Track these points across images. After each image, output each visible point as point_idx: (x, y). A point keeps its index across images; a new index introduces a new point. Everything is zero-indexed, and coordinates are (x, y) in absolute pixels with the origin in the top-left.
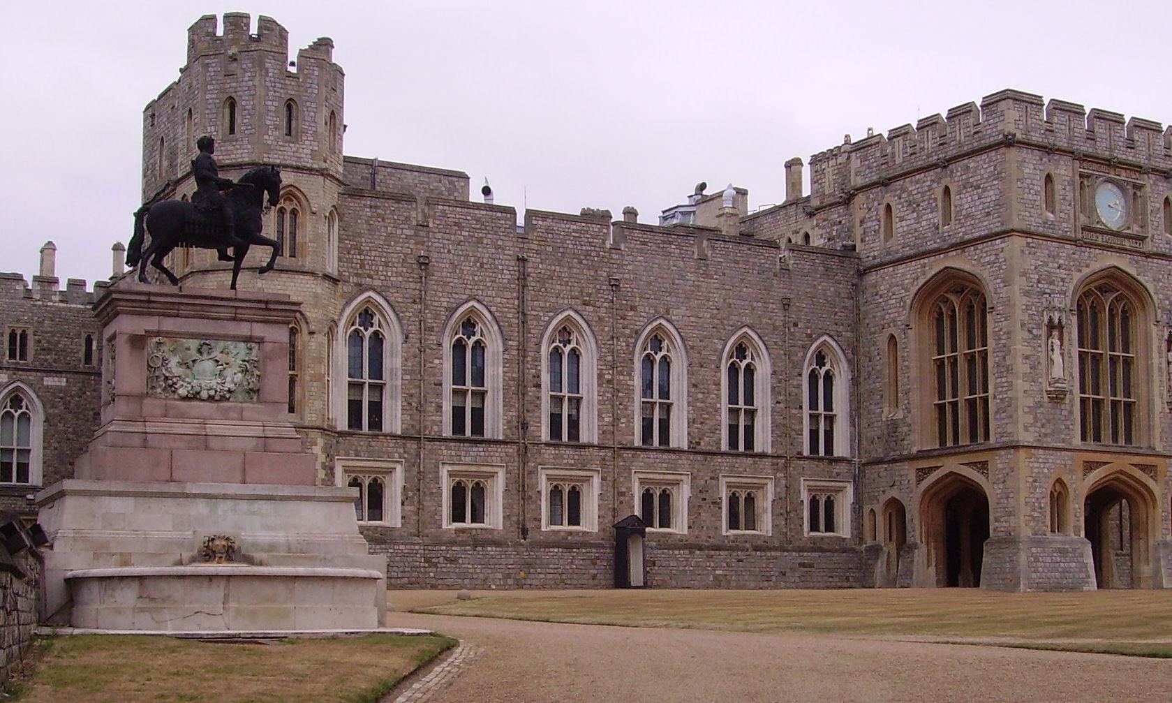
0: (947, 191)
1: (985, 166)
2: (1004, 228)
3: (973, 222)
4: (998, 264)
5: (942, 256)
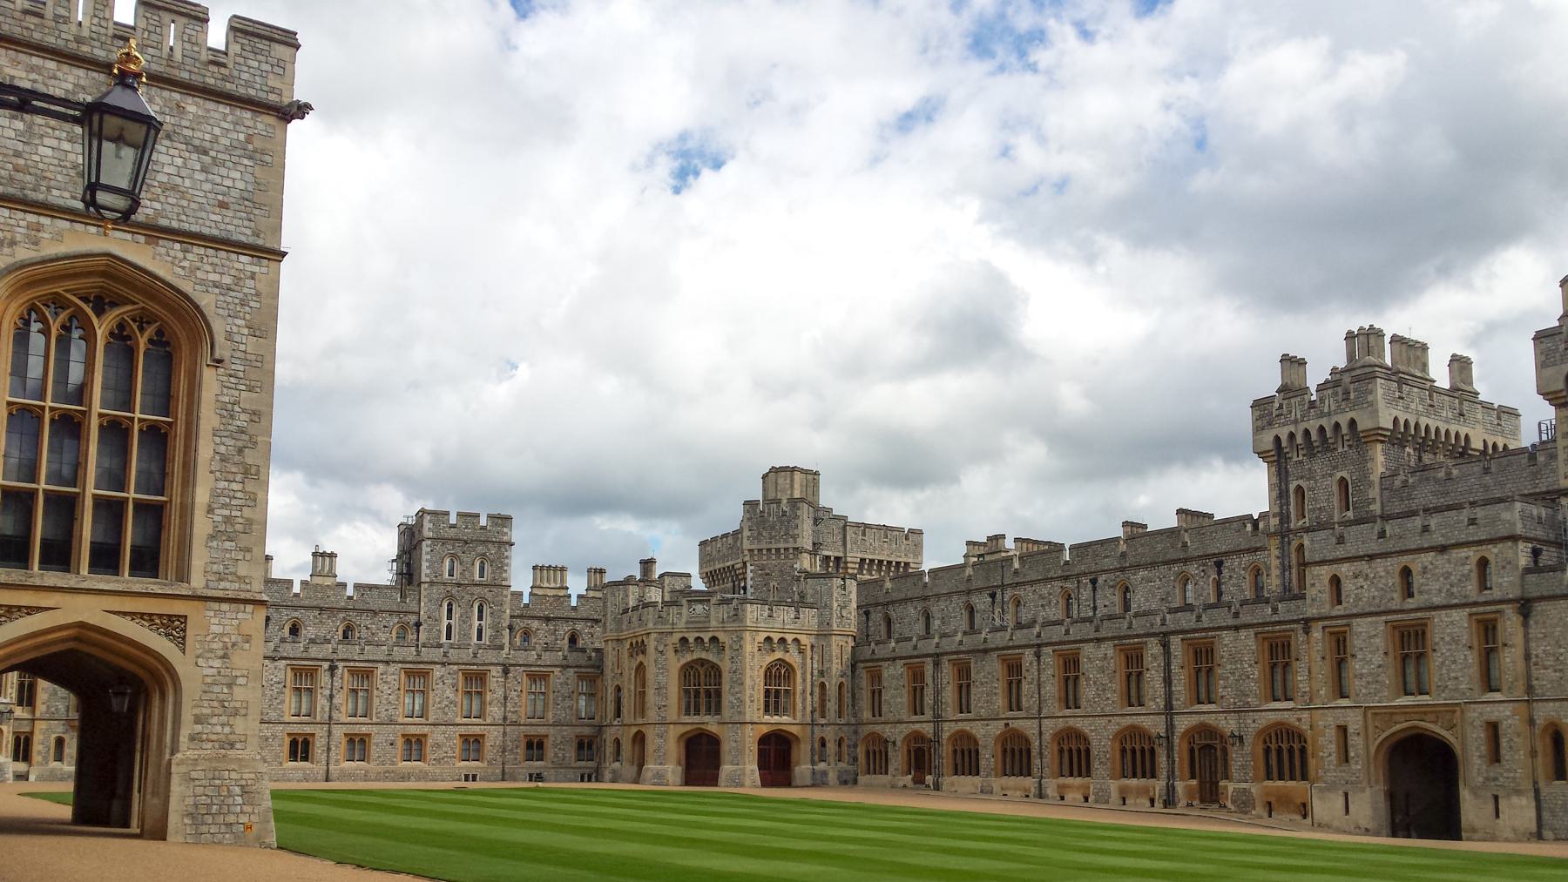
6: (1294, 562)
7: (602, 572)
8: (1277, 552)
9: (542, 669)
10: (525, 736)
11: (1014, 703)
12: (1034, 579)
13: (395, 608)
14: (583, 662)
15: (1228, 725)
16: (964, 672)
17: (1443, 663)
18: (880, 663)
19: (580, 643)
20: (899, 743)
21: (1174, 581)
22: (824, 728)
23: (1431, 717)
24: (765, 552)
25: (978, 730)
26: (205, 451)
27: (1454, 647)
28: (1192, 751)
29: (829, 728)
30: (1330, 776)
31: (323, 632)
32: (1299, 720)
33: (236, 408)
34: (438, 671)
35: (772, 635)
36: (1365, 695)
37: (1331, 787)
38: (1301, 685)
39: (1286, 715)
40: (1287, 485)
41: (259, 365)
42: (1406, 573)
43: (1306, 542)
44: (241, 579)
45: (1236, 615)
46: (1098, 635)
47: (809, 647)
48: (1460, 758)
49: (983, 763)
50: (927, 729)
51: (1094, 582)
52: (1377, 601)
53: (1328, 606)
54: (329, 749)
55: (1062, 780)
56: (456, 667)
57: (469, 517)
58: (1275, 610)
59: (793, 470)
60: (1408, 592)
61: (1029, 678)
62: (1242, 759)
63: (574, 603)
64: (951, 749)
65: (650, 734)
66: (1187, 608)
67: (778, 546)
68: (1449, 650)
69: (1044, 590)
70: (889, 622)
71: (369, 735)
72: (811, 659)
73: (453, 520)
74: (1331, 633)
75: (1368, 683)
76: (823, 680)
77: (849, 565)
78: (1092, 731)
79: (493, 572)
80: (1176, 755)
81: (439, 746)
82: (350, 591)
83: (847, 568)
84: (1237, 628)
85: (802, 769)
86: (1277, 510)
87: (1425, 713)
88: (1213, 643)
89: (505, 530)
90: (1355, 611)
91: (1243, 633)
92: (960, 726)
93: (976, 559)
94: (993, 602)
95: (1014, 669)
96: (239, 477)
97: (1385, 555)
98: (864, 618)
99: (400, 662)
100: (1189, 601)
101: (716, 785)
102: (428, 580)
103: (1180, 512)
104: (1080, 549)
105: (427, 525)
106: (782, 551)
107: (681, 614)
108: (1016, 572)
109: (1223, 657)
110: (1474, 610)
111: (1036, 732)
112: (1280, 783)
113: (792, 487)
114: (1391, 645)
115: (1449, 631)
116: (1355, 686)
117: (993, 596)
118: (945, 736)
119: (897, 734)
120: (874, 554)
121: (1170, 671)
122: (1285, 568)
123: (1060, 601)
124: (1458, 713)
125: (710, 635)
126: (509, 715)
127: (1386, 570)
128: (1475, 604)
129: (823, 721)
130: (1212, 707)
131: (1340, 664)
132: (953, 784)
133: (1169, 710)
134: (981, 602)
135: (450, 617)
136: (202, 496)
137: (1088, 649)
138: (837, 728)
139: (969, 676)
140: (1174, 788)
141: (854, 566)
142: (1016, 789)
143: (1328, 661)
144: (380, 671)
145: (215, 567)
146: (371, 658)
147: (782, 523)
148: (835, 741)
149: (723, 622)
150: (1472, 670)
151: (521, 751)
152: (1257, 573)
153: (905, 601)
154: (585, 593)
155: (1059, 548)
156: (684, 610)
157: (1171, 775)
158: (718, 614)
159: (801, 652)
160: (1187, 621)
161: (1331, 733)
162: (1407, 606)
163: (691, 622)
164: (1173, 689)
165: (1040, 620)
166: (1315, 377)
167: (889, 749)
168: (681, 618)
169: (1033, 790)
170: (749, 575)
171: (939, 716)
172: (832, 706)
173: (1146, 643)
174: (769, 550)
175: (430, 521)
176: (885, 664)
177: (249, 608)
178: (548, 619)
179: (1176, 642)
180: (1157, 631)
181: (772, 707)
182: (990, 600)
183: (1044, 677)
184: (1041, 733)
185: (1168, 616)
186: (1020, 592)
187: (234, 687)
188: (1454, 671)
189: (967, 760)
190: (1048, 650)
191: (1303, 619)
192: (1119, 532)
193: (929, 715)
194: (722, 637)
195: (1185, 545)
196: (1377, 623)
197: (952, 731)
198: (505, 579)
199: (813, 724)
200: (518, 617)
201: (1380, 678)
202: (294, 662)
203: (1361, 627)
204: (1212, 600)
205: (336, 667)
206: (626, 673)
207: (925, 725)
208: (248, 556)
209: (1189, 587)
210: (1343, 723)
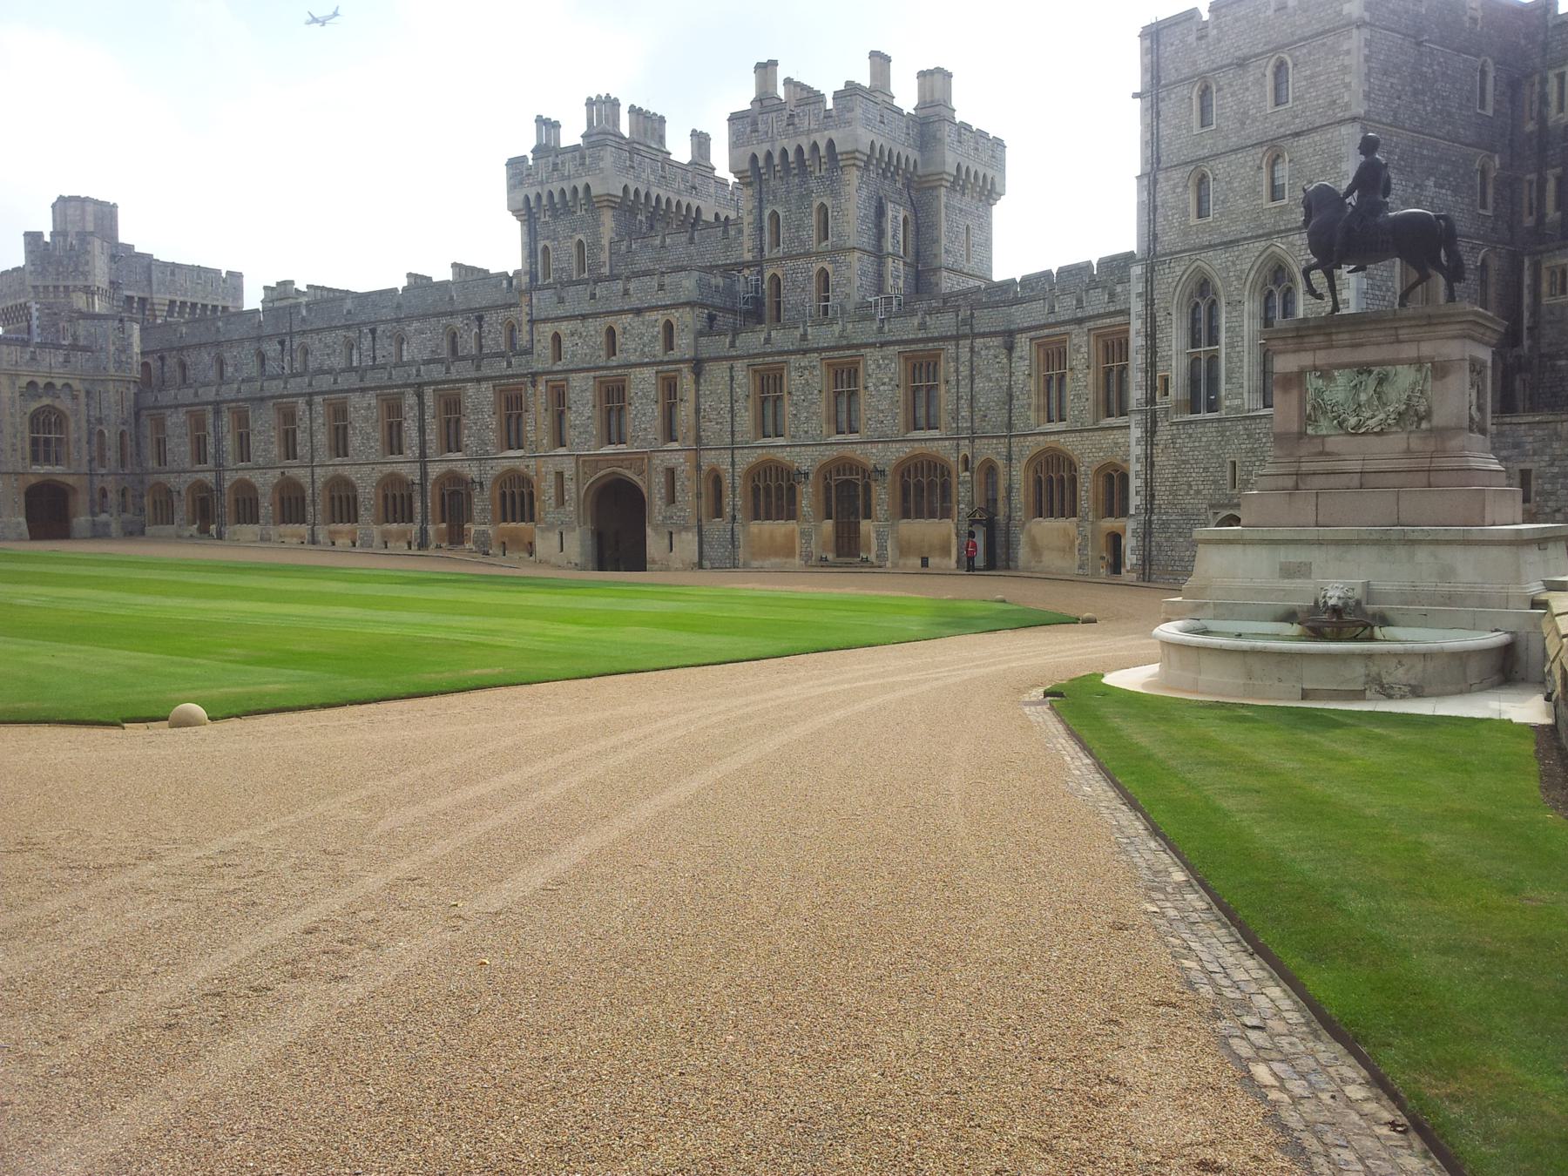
11: (290, 452)
12: (321, 325)
15: (471, 471)
20: (183, 493)
21: (443, 334)
22: (105, 477)
25: (256, 478)
27: (644, 401)
29: (110, 478)
30: (550, 518)
32: (528, 466)
36: (578, 444)
39: (517, 462)
40: (536, 244)
42: (611, 332)
45: (478, 368)
46: (362, 385)
49: (262, 511)
50: (210, 478)
51: (373, 331)
53: (550, 361)
55: (333, 527)
58: (509, 365)
60: (612, 350)
62: (482, 503)
69: (329, 338)
74: (553, 387)
76: (100, 427)
84: (478, 380)
87: (622, 460)
90: (571, 367)
91: (484, 385)
92: (240, 475)
94: (283, 350)
95: (289, 417)
97: (595, 315)
98: (159, 363)
103: (455, 265)
108: (304, 320)
109: (467, 408)
111: (309, 480)
112: (513, 525)
116: (570, 435)
117: (282, 343)
118: (227, 485)
121: (424, 420)
127: (597, 327)
128: (661, 363)
130: (458, 455)
131: (559, 418)
133: (423, 458)
134: (271, 349)
137: (354, 399)
138: (118, 477)
139: (247, 426)
140: (426, 531)
142: (292, 536)
148: (117, 491)
150: (656, 422)
152: (512, 329)
157: (425, 520)
160: (437, 372)
161: (551, 478)
166: (572, 134)
171: (221, 465)
172: (112, 454)
173: (403, 393)
176: (168, 412)
182: (279, 347)
183: (315, 429)
184: (313, 482)
188: (644, 423)
189: (247, 510)
190: (318, 399)
191: (531, 373)
193: (211, 463)
195: (451, 298)
197: (233, 480)
203: (576, 381)
207: (207, 474)
210: (560, 470)
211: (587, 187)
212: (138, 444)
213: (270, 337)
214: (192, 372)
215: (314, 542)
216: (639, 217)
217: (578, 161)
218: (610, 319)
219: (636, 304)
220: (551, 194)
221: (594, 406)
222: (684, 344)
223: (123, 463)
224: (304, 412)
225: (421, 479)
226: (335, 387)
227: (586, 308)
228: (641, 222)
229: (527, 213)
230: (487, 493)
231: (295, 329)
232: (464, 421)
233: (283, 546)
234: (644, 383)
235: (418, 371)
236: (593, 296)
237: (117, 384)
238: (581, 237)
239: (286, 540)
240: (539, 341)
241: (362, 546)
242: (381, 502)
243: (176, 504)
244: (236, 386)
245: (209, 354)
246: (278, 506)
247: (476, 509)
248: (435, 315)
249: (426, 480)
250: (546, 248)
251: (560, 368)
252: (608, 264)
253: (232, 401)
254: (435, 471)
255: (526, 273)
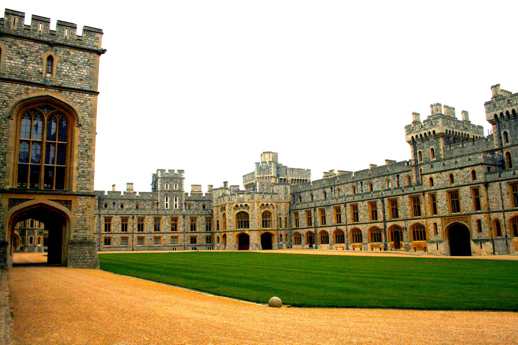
0: (50, 59)
1: (81, 57)
2: (92, 90)
3: (70, 80)
4: (86, 105)
5: (43, 89)
6: (420, 174)
7: (212, 186)
8: (415, 171)
9: (194, 216)
10: (190, 236)
12: (344, 183)
13: (151, 199)
14: (207, 214)
15: (402, 224)
16: (323, 212)
17: (463, 203)
18: (298, 211)
19: (206, 208)
20: (304, 235)
21: (385, 181)
22: (282, 231)
23: (460, 219)
24: (262, 178)
25: (328, 230)
26: (76, 151)
27: (466, 197)
28: (392, 233)
29: (283, 231)
30: (432, 239)
31: (130, 206)
32: (423, 222)
33: (85, 138)
34: (164, 217)
35: (264, 203)
37: (433, 242)
38: (423, 211)
40: (416, 150)
41: (92, 125)
42: (451, 176)
43: (422, 168)
44: (87, 189)
45: (403, 191)
46: (363, 199)
47: (275, 207)
48: (470, 231)
49: (330, 240)
50: (313, 230)
51: (361, 183)
52: (443, 185)
53: (429, 187)
54: (133, 241)
55: (353, 244)
56: (169, 216)
57: (171, 171)
58: (414, 189)
59: (271, 152)
60: (452, 181)
61: (343, 213)
62: (407, 235)
63: (204, 195)
64: (320, 236)
65: (227, 234)
66: (389, 189)
67: (266, 176)
68: (465, 198)
69: (347, 186)
70: (300, 198)
71: (144, 237)
72: (277, 210)
73: (167, 172)
74: (431, 195)
75: (442, 210)
76: (280, 216)
77: (288, 181)
78: (362, 228)
79: (179, 187)
80: (387, 235)
81: (165, 240)
82: (138, 194)
83: (288, 182)
84: (403, 195)
85: (275, 244)
86: (414, 159)
87: (459, 218)
88: (397, 200)
89: (182, 174)
90: (437, 188)
91: (405, 196)
93: (326, 177)
94: (332, 190)
95: (338, 210)
96: (86, 159)
97: (445, 171)
98: (293, 197)
99: (152, 215)
100: (390, 187)
101: (248, 250)
102: (160, 190)
103: (386, 160)
104: (357, 173)
105: (159, 174)
106: (267, 177)
107: (235, 198)
110: (472, 186)
111: (345, 229)
112: (418, 241)
113: (269, 158)
114: (448, 198)
115: (464, 193)
116: (439, 210)
117: (331, 188)
118: (318, 232)
119: (303, 232)
120: (296, 177)
121: (384, 209)
122: (417, 176)
123: (352, 189)
124: (469, 218)
125: (245, 204)
126: (185, 230)
127: (445, 175)
128: (472, 184)
129: (281, 229)
132: (321, 247)
133: (385, 221)
134: (328, 190)
135: (167, 201)
136: (75, 165)
137: (360, 203)
138: (285, 231)
139: (325, 214)
140: (387, 245)
141: (290, 181)
142: (340, 247)
143: (430, 204)
144: (146, 218)
145: (79, 186)
146: (144, 214)
147: (267, 169)
149: (249, 200)
151: (189, 241)
152: (409, 178)
153: (305, 191)
154: (207, 192)
155: (350, 173)
156: (236, 196)
157: (386, 241)
158: (247, 197)
159: (273, 208)
160: (389, 193)
161: (432, 226)
162: (452, 186)
163: (239, 200)
164: (386, 214)
165: (346, 195)
167: (302, 237)
168: (235, 199)
169: (345, 248)
170: (258, 185)
172: (283, 224)
173: (377, 201)
174: (263, 177)
175: (160, 172)
176: (299, 211)
177: (90, 198)
178: (196, 201)
179: (386, 200)
180: (380, 197)
181: (265, 226)
182: (330, 190)
183: (347, 214)
184: (347, 230)
185: (383, 192)
186: (340, 187)
187: (86, 221)
189: (325, 239)
190: (348, 204)
191: (423, 191)
192: (369, 167)
194: (248, 204)
195: (388, 171)
196: (444, 191)
198: (183, 189)
199: (278, 230)
200: (188, 200)
201: (445, 208)
202: (122, 216)
203: (439, 193)
204: (397, 186)
205: (134, 217)
206: (220, 216)
207: (312, 229)
208: (89, 182)
209: (390, 183)
210: (435, 222)
211: (434, 132)
212: (290, 221)
213: (327, 187)
214: (303, 199)
215: (348, 249)
216: (451, 139)
217: (430, 124)
218: (451, 172)
219: (461, 166)
220: (421, 135)
221: (447, 201)
222: (480, 177)
223: (286, 227)
224: (343, 209)
225: (384, 227)
226: (353, 200)
227: (442, 169)
228: (451, 141)
229: (413, 142)
230: (408, 231)
231: (336, 184)
232: (399, 208)
233: (337, 250)
234: (465, 193)
235: (382, 193)
236: (444, 165)
237: (285, 203)
238: (433, 147)
239: (338, 249)
240: (425, 181)
241: (364, 250)
242: (370, 235)
243: (302, 239)
244: (320, 202)
245: (308, 193)
246: (335, 238)
247: (404, 237)
248: (382, 176)
249: (386, 228)
250: (420, 152)
251: (433, 189)
252: (443, 155)
253: (320, 207)
254: (389, 225)
255: (413, 160)
